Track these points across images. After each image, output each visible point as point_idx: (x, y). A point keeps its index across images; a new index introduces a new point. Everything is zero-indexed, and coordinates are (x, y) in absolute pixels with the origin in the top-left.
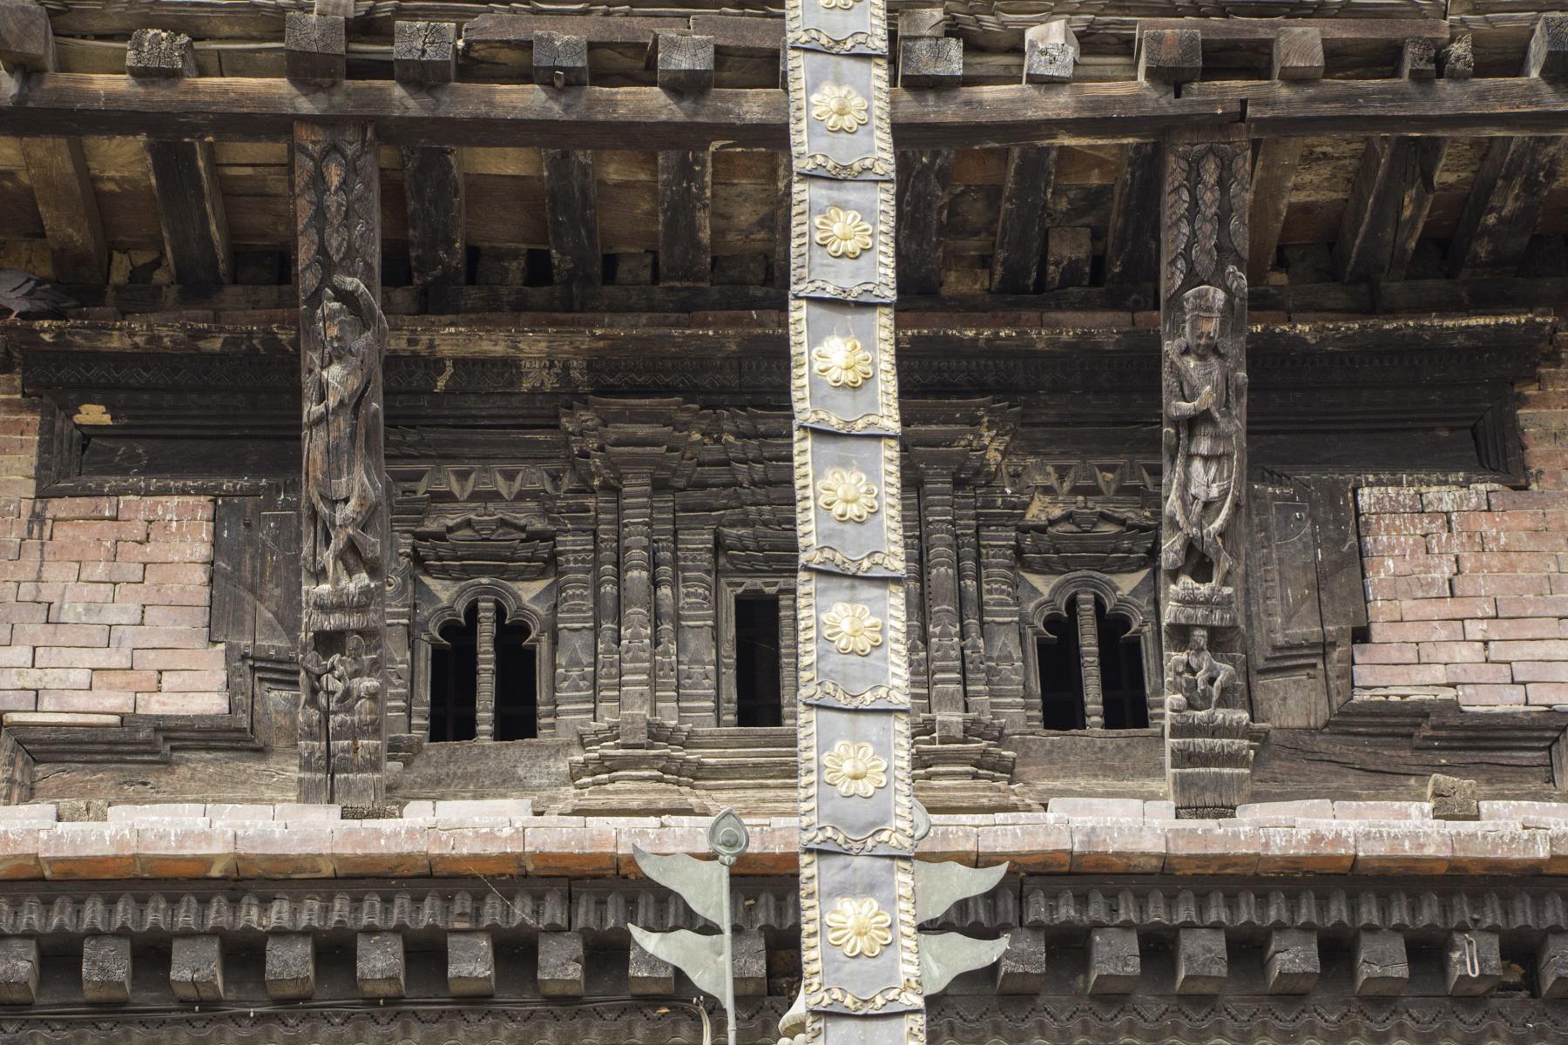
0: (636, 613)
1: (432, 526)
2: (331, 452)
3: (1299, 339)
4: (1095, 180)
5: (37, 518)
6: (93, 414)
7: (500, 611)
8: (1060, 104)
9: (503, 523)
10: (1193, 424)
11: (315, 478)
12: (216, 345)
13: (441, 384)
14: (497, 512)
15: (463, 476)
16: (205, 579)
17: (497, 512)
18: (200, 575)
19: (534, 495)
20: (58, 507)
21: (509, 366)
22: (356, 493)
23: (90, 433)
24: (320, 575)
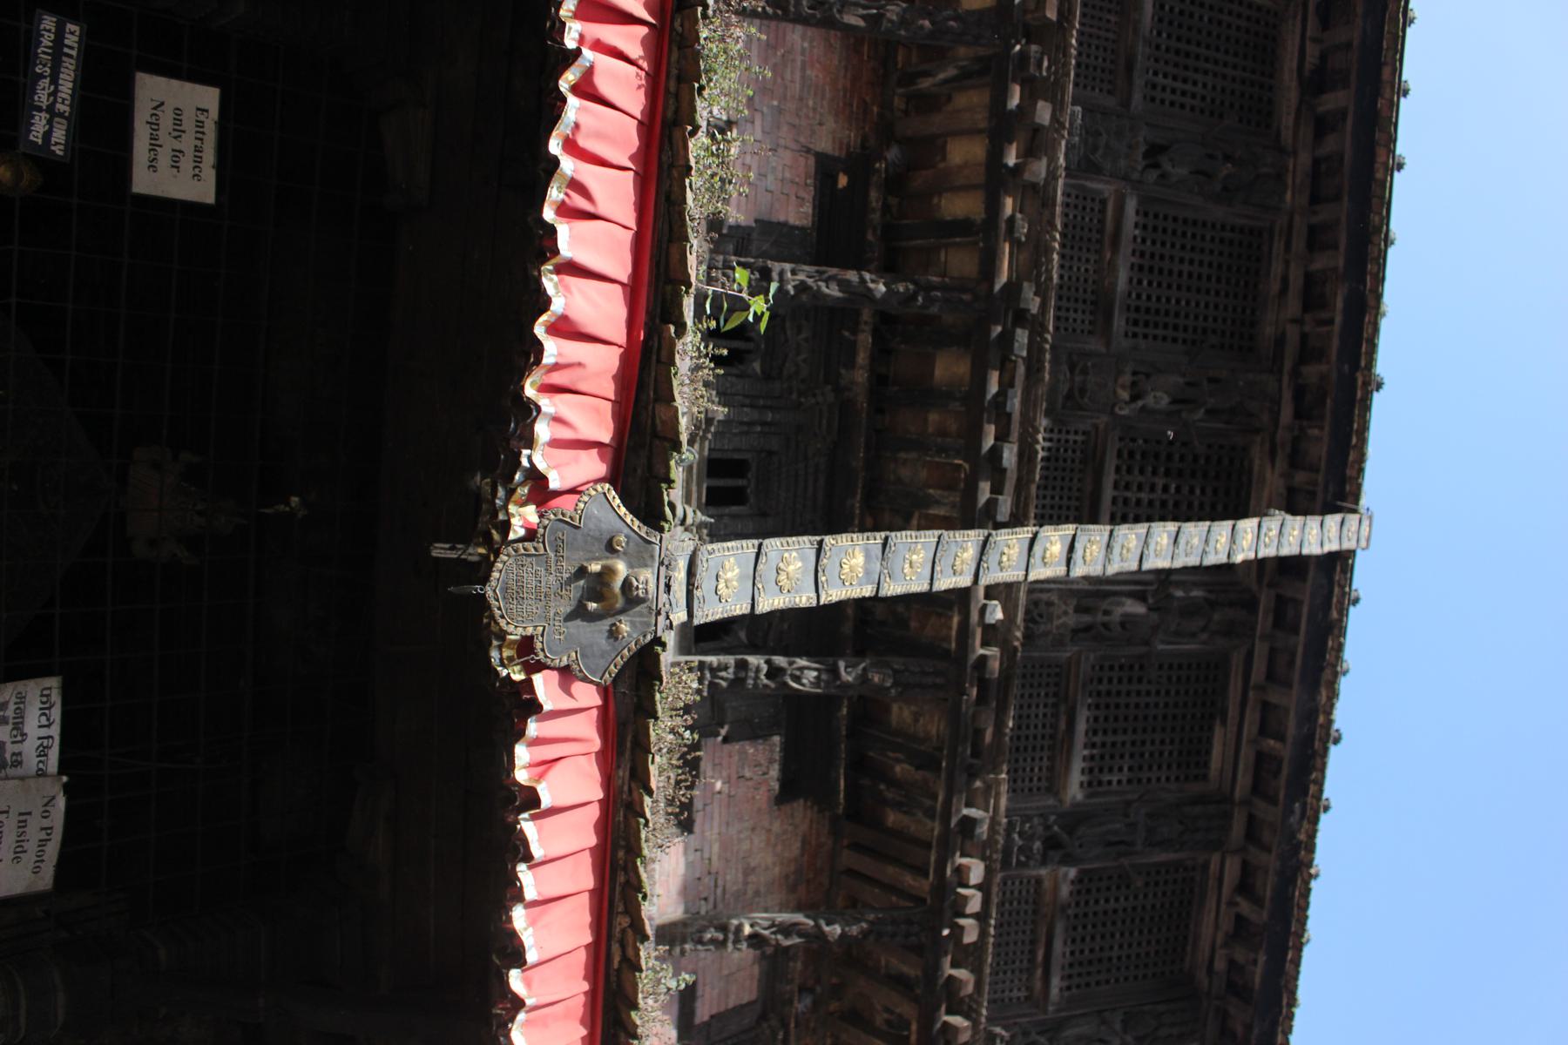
0: (755, 415)
1: (788, 324)
3: (840, 709)
4: (913, 624)
5: (808, 151)
6: (843, 181)
7: (749, 352)
8: (975, 617)
10: (834, 671)
12: (870, 237)
13: (846, 334)
15: (806, 340)
18: (782, 218)
20: (812, 161)
21: (851, 364)
23: (836, 182)
24: (794, 272)
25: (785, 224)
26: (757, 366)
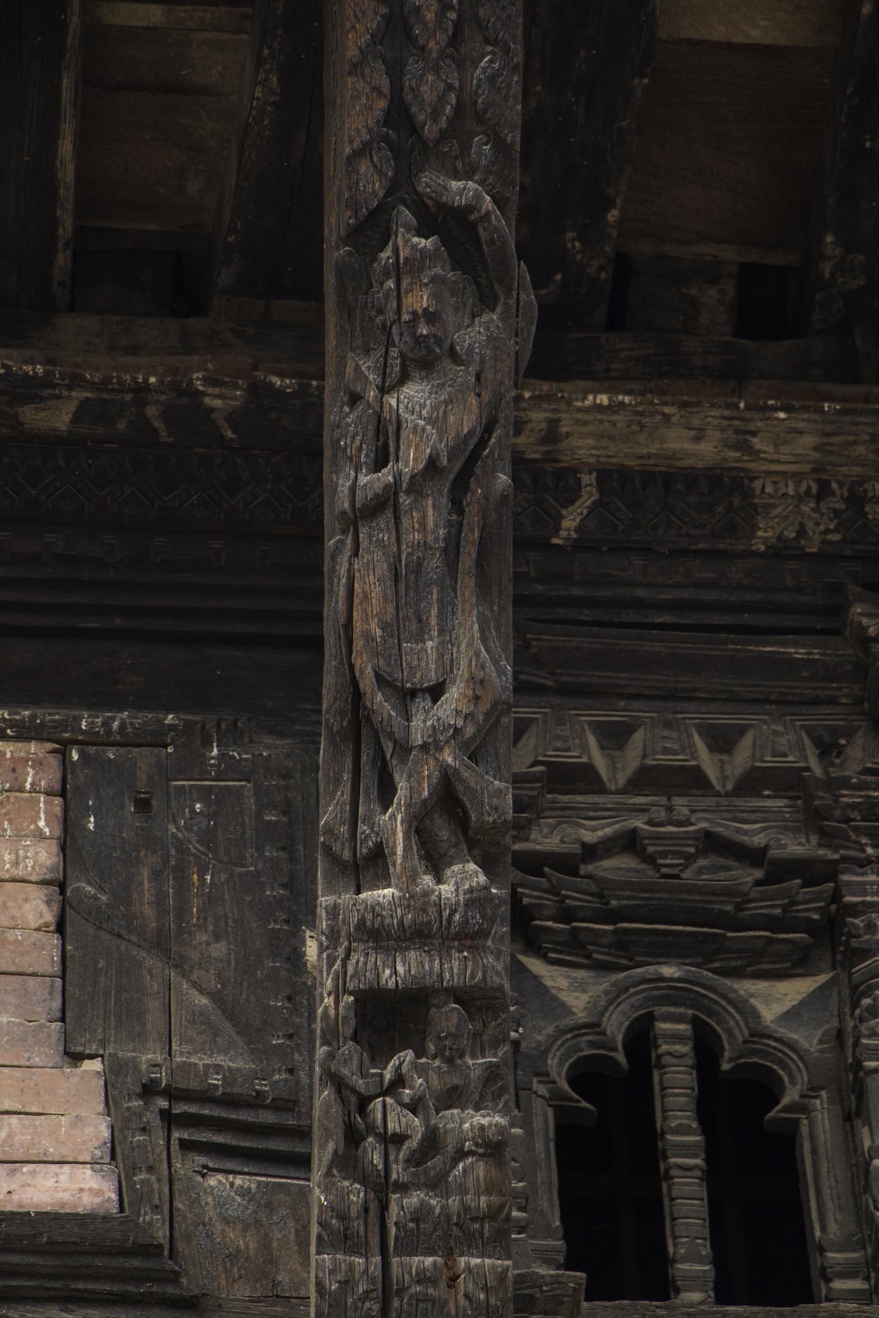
2: (403, 577)
9: (712, 843)
11: (368, 636)
14: (697, 816)
16: (49, 917)
17: (697, 816)
19: (788, 782)
22: (462, 670)
25: (58, 884)
26: (775, 1000)
